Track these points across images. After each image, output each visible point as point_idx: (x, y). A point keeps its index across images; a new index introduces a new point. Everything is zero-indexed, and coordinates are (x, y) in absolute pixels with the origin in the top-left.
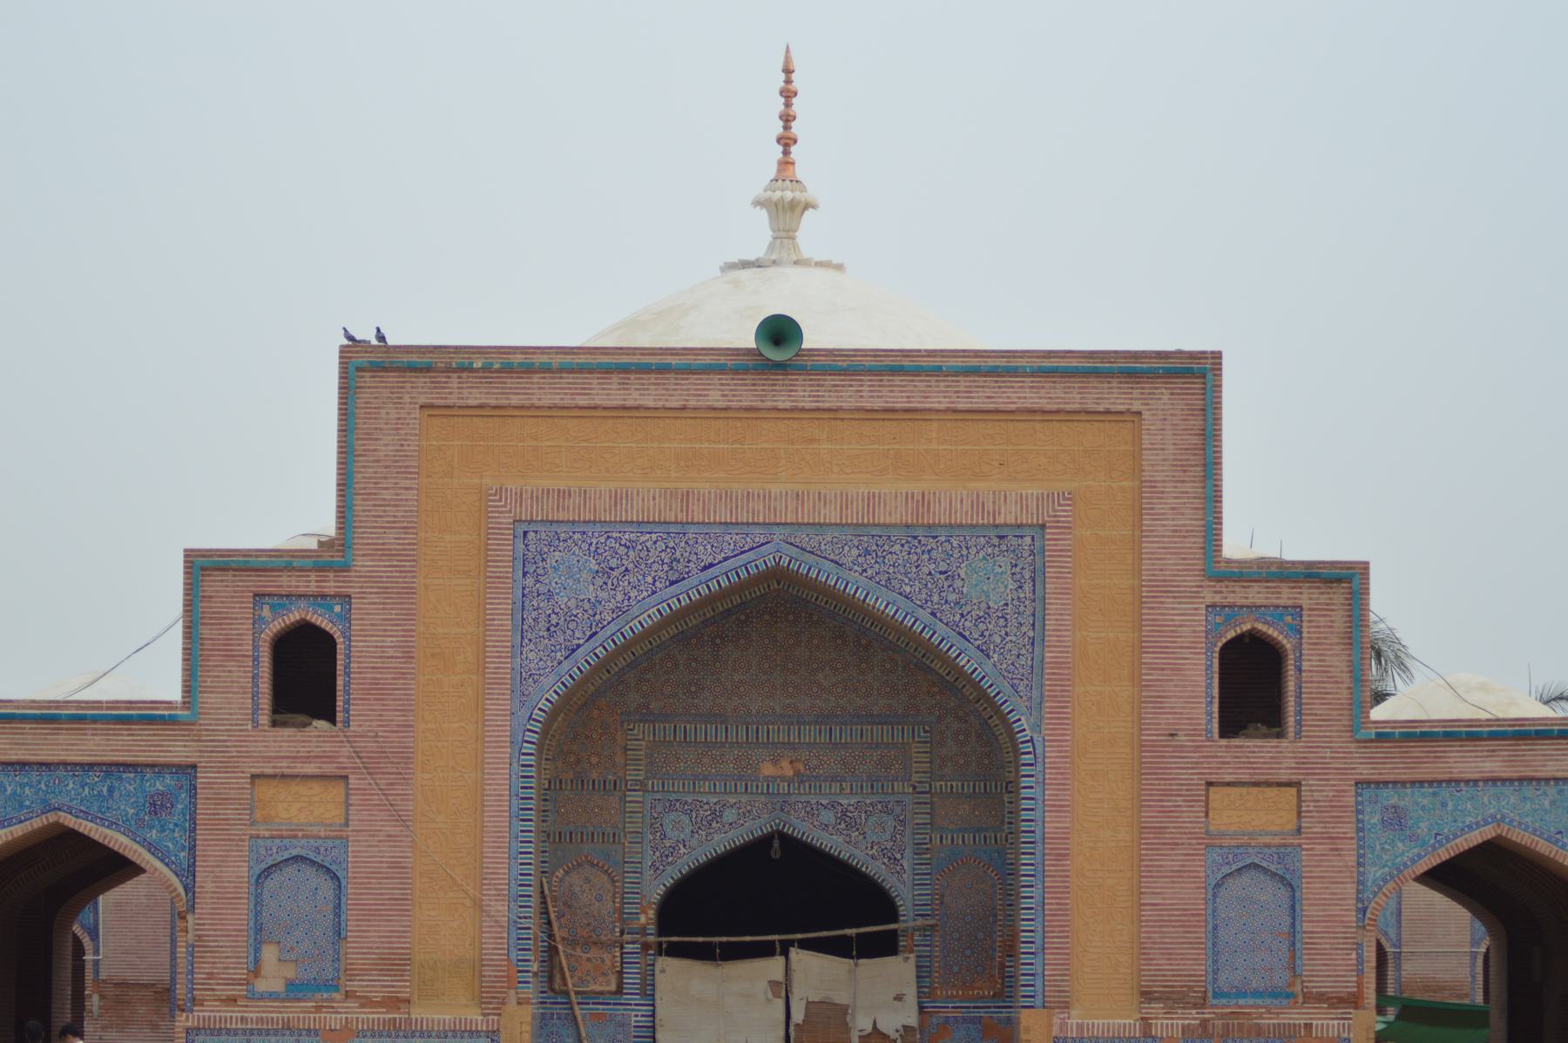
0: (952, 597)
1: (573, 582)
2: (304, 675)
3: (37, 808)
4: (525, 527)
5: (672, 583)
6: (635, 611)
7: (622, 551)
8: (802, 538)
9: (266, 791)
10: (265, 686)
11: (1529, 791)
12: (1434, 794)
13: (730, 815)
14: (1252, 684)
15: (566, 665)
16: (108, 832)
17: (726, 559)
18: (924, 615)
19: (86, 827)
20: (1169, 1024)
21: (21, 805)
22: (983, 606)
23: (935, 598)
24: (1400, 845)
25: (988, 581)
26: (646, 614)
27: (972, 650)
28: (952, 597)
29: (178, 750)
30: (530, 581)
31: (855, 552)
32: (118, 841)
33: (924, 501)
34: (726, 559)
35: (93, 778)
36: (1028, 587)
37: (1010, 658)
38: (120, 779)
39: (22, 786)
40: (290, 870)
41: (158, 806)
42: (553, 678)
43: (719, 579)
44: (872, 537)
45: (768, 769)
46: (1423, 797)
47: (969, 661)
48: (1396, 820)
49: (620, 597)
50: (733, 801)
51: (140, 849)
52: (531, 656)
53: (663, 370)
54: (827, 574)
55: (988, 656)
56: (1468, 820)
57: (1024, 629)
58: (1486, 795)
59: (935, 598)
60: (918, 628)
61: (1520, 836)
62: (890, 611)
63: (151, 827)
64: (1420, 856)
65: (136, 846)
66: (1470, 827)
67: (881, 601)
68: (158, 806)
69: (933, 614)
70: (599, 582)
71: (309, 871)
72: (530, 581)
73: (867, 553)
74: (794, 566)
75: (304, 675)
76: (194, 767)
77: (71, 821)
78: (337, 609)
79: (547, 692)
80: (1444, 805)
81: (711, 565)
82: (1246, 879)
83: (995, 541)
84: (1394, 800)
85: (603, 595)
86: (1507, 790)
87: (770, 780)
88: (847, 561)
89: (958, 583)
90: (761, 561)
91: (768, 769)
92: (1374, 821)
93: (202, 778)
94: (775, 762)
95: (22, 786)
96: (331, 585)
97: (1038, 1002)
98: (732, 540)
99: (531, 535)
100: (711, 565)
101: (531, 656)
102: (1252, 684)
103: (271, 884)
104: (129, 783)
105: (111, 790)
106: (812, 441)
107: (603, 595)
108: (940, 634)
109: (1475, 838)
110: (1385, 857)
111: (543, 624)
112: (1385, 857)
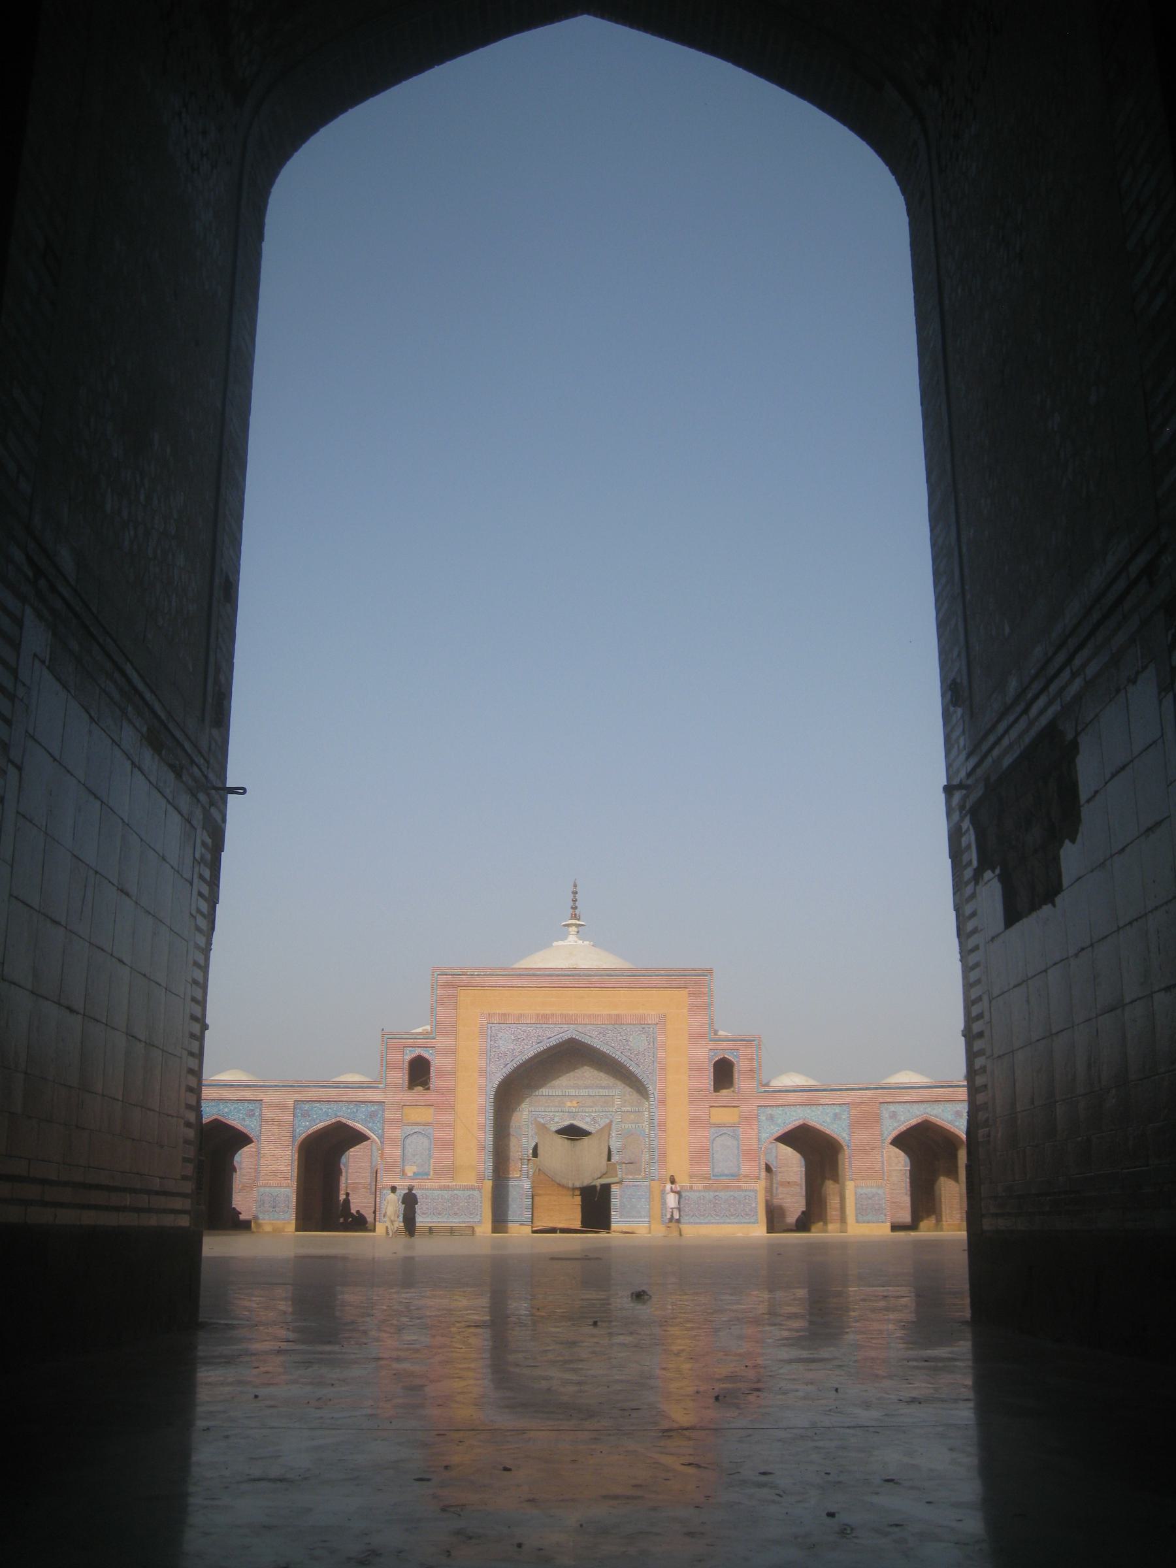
2: (419, 1072)
9: (406, 1110)
10: (406, 1077)
11: (814, 1108)
13: (556, 1119)
14: (723, 1074)
19: (349, 1123)
20: (699, 1185)
26: (531, 1054)
29: (376, 1096)
32: (359, 1126)
41: (372, 1115)
43: (553, 1042)
45: (569, 1104)
46: (779, 1110)
48: (771, 1118)
58: (800, 1110)
61: (812, 1123)
67: (605, 1049)
71: (421, 1137)
75: (419, 1072)
77: (344, 1120)
82: (723, 1137)
86: (807, 1108)
90: (567, 1036)
91: (569, 1104)
102: (723, 1074)
103: (408, 1141)
108: (623, 1059)
109: (797, 1123)
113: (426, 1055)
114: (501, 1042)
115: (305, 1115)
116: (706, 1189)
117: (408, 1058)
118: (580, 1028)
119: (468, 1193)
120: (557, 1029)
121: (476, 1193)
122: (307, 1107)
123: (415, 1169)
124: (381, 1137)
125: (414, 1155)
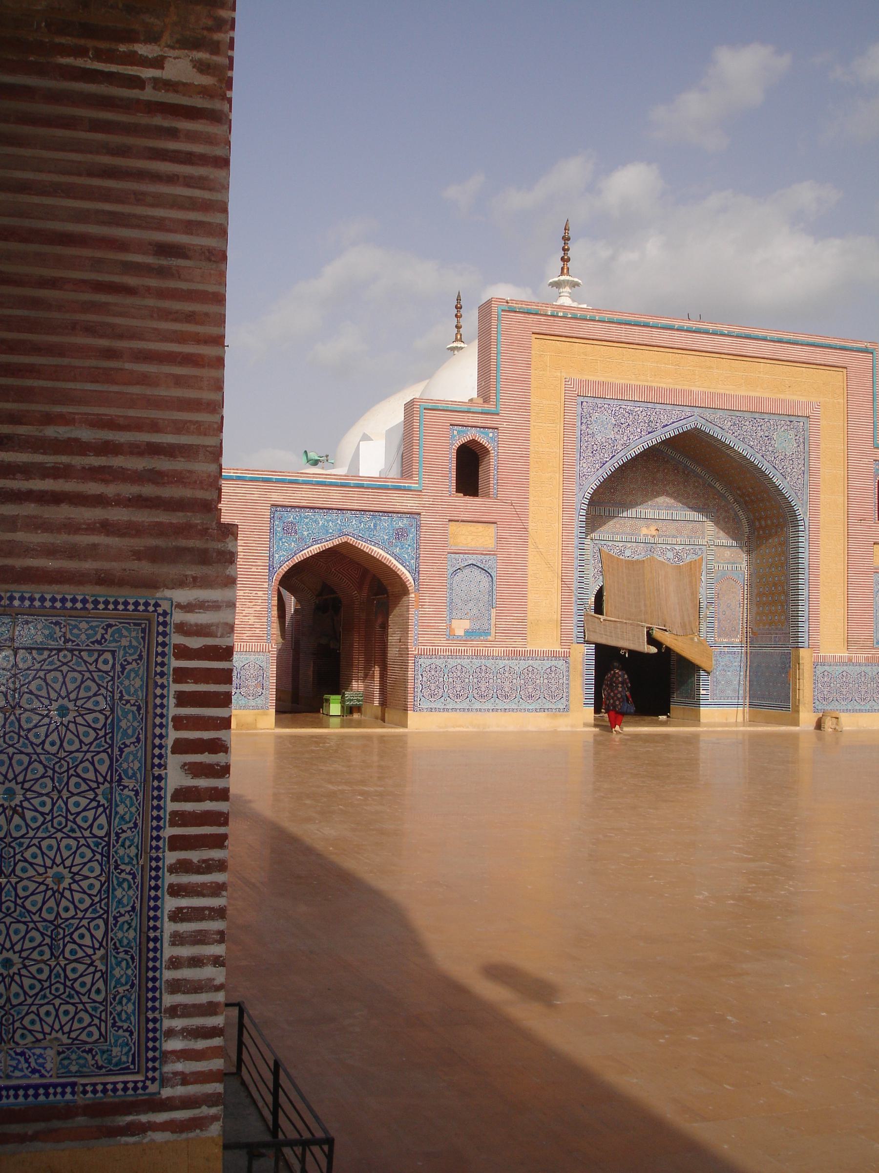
1: (604, 428)
2: (470, 468)
3: (336, 534)
4: (582, 399)
5: (649, 433)
6: (632, 446)
7: (627, 415)
8: (707, 414)
15: (601, 471)
16: (373, 547)
18: (759, 456)
20: (861, 656)
21: (327, 531)
23: (764, 449)
25: (785, 442)
27: (779, 475)
28: (770, 449)
30: (584, 427)
31: (729, 424)
33: (759, 400)
35: (366, 518)
36: (802, 446)
37: (795, 480)
38: (380, 520)
39: (328, 521)
40: (467, 571)
41: (400, 534)
42: (594, 477)
44: (757, 415)
45: (644, 531)
47: (777, 480)
49: (625, 438)
51: (391, 558)
52: (584, 465)
54: (717, 433)
59: (764, 449)
60: (756, 462)
62: (745, 453)
63: (397, 546)
65: (388, 556)
68: (400, 534)
70: (616, 430)
72: (584, 427)
73: (735, 424)
74: (703, 428)
75: (470, 468)
76: (419, 514)
78: (491, 435)
79: (592, 484)
81: (667, 425)
83: (788, 423)
85: (618, 437)
89: (773, 442)
91: (644, 531)
93: (424, 519)
94: (648, 527)
95: (328, 521)
96: (489, 421)
97: (806, 644)
98: (676, 413)
99: (584, 404)
100: (667, 425)
101: (584, 465)
104: (385, 522)
105: (375, 525)
106: (710, 367)
107: (618, 437)
108: (765, 466)
111: (590, 450)
113: (483, 441)
114: (594, 428)
115: (290, 529)
116: (869, 662)
117: (458, 444)
118: (707, 414)
119: (548, 664)
120: (676, 413)
121: (560, 663)
122: (291, 517)
123: (466, 624)
124: (416, 572)
125: (466, 602)
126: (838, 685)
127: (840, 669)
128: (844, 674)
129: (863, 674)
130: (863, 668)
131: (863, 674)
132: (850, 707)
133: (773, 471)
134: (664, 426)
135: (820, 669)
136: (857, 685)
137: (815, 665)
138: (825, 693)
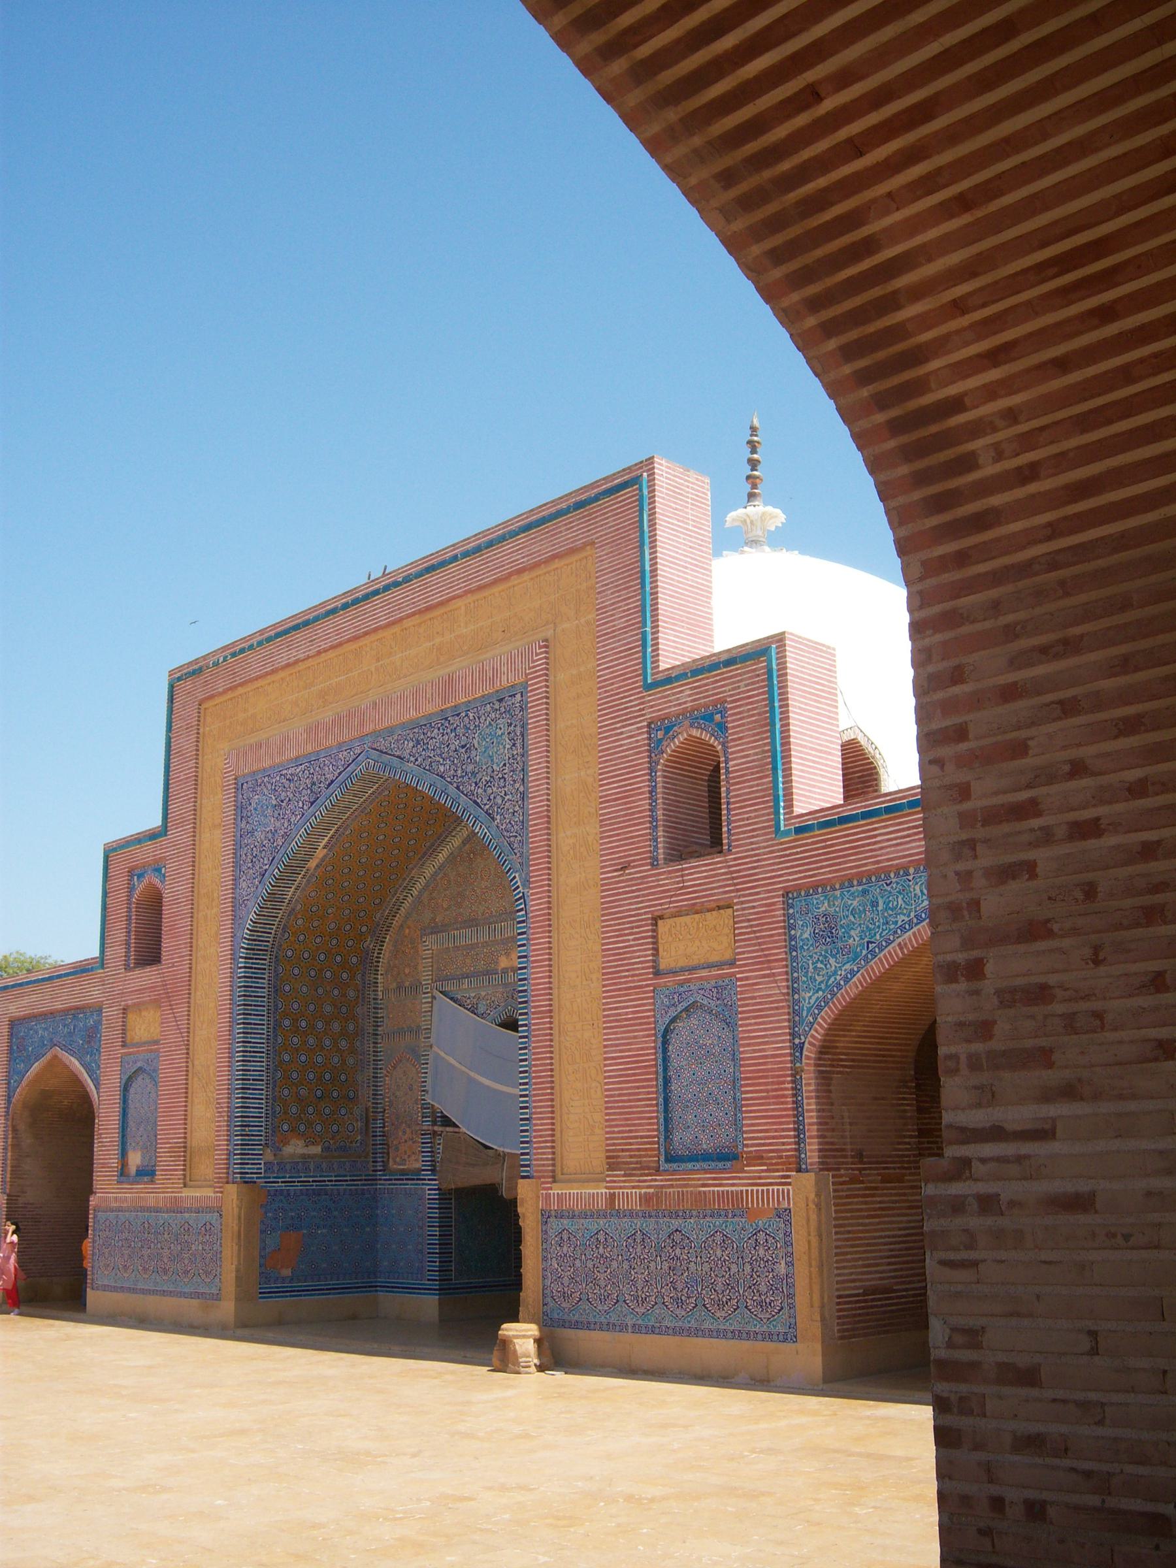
0: (470, 768)
12: (864, 892)
17: (340, 774)
18: (452, 789)
20: (631, 1192)
22: (490, 770)
24: (832, 961)
31: (411, 744)
34: (340, 774)
48: (828, 932)
50: (483, 994)
53: (306, 623)
55: (493, 819)
56: (901, 918)
57: (517, 785)
64: (853, 973)
66: (902, 928)
69: (458, 788)
73: (418, 743)
80: (875, 904)
81: (332, 782)
84: (824, 907)
85: (278, 824)
87: (505, 971)
88: (406, 754)
92: (806, 935)
94: (507, 955)
100: (332, 782)
107: (278, 824)
110: (819, 979)
112: (819, 979)
126: (590, 1264)
127: (593, 1225)
128: (601, 1237)
129: (639, 1237)
130: (638, 1222)
131: (639, 1237)
132: (613, 1318)
133: (473, 809)
134: (329, 785)
135: (555, 1225)
136: (626, 1265)
137: (546, 1216)
138: (566, 1281)
